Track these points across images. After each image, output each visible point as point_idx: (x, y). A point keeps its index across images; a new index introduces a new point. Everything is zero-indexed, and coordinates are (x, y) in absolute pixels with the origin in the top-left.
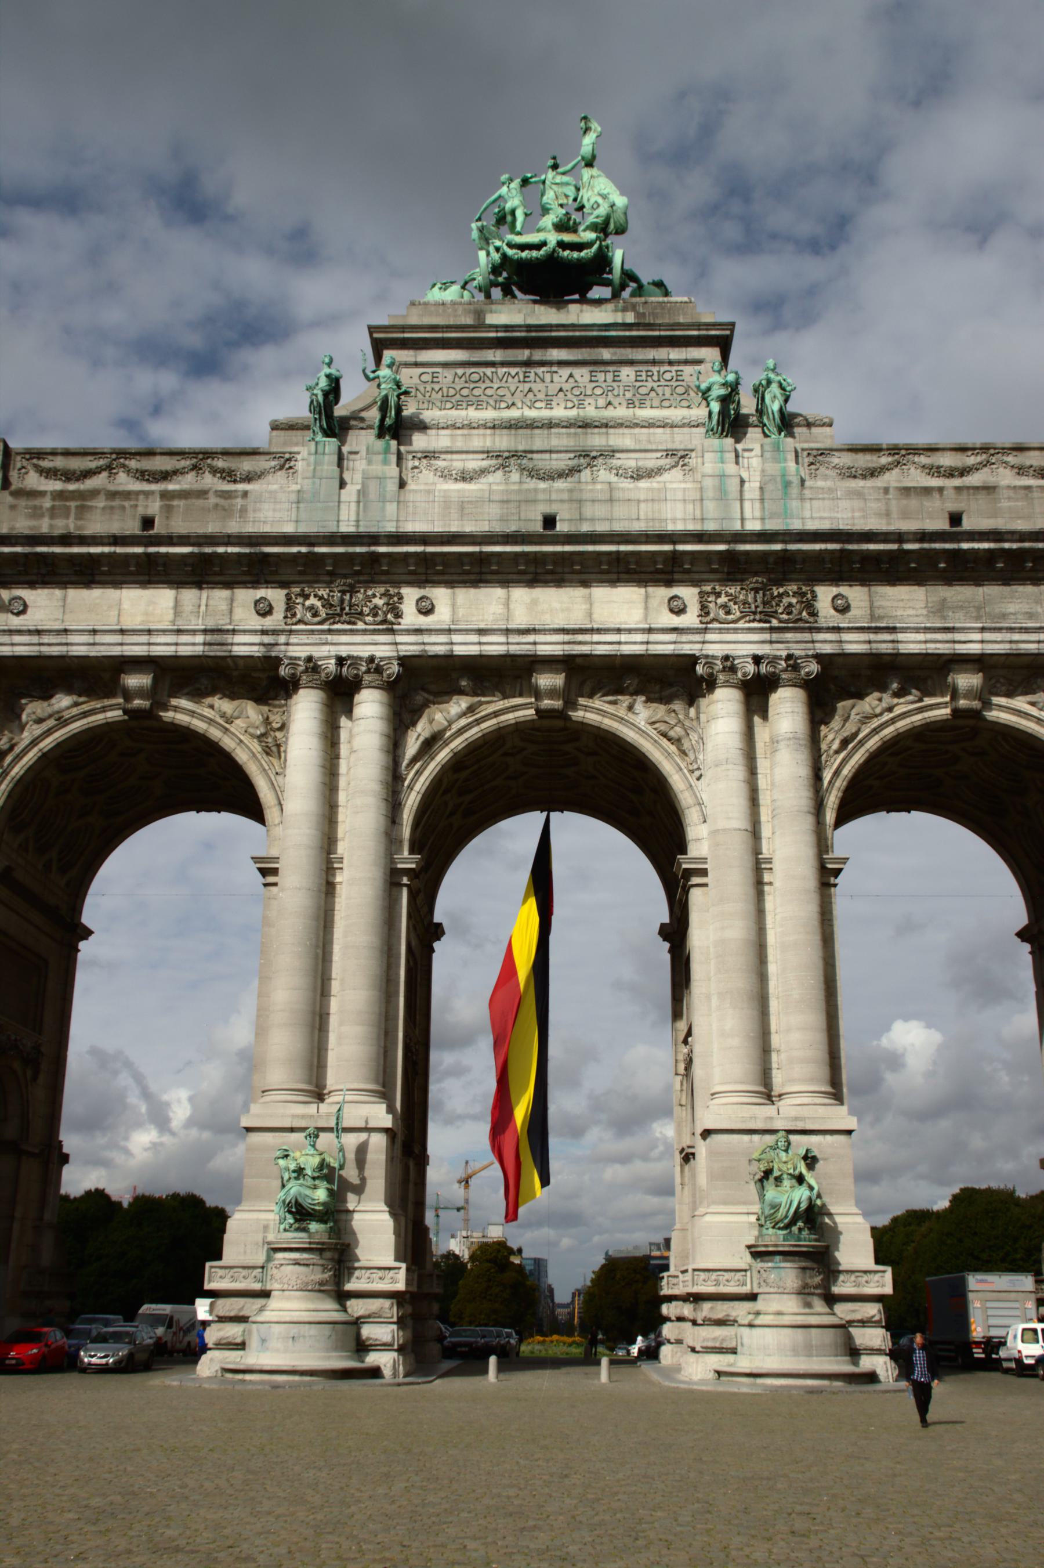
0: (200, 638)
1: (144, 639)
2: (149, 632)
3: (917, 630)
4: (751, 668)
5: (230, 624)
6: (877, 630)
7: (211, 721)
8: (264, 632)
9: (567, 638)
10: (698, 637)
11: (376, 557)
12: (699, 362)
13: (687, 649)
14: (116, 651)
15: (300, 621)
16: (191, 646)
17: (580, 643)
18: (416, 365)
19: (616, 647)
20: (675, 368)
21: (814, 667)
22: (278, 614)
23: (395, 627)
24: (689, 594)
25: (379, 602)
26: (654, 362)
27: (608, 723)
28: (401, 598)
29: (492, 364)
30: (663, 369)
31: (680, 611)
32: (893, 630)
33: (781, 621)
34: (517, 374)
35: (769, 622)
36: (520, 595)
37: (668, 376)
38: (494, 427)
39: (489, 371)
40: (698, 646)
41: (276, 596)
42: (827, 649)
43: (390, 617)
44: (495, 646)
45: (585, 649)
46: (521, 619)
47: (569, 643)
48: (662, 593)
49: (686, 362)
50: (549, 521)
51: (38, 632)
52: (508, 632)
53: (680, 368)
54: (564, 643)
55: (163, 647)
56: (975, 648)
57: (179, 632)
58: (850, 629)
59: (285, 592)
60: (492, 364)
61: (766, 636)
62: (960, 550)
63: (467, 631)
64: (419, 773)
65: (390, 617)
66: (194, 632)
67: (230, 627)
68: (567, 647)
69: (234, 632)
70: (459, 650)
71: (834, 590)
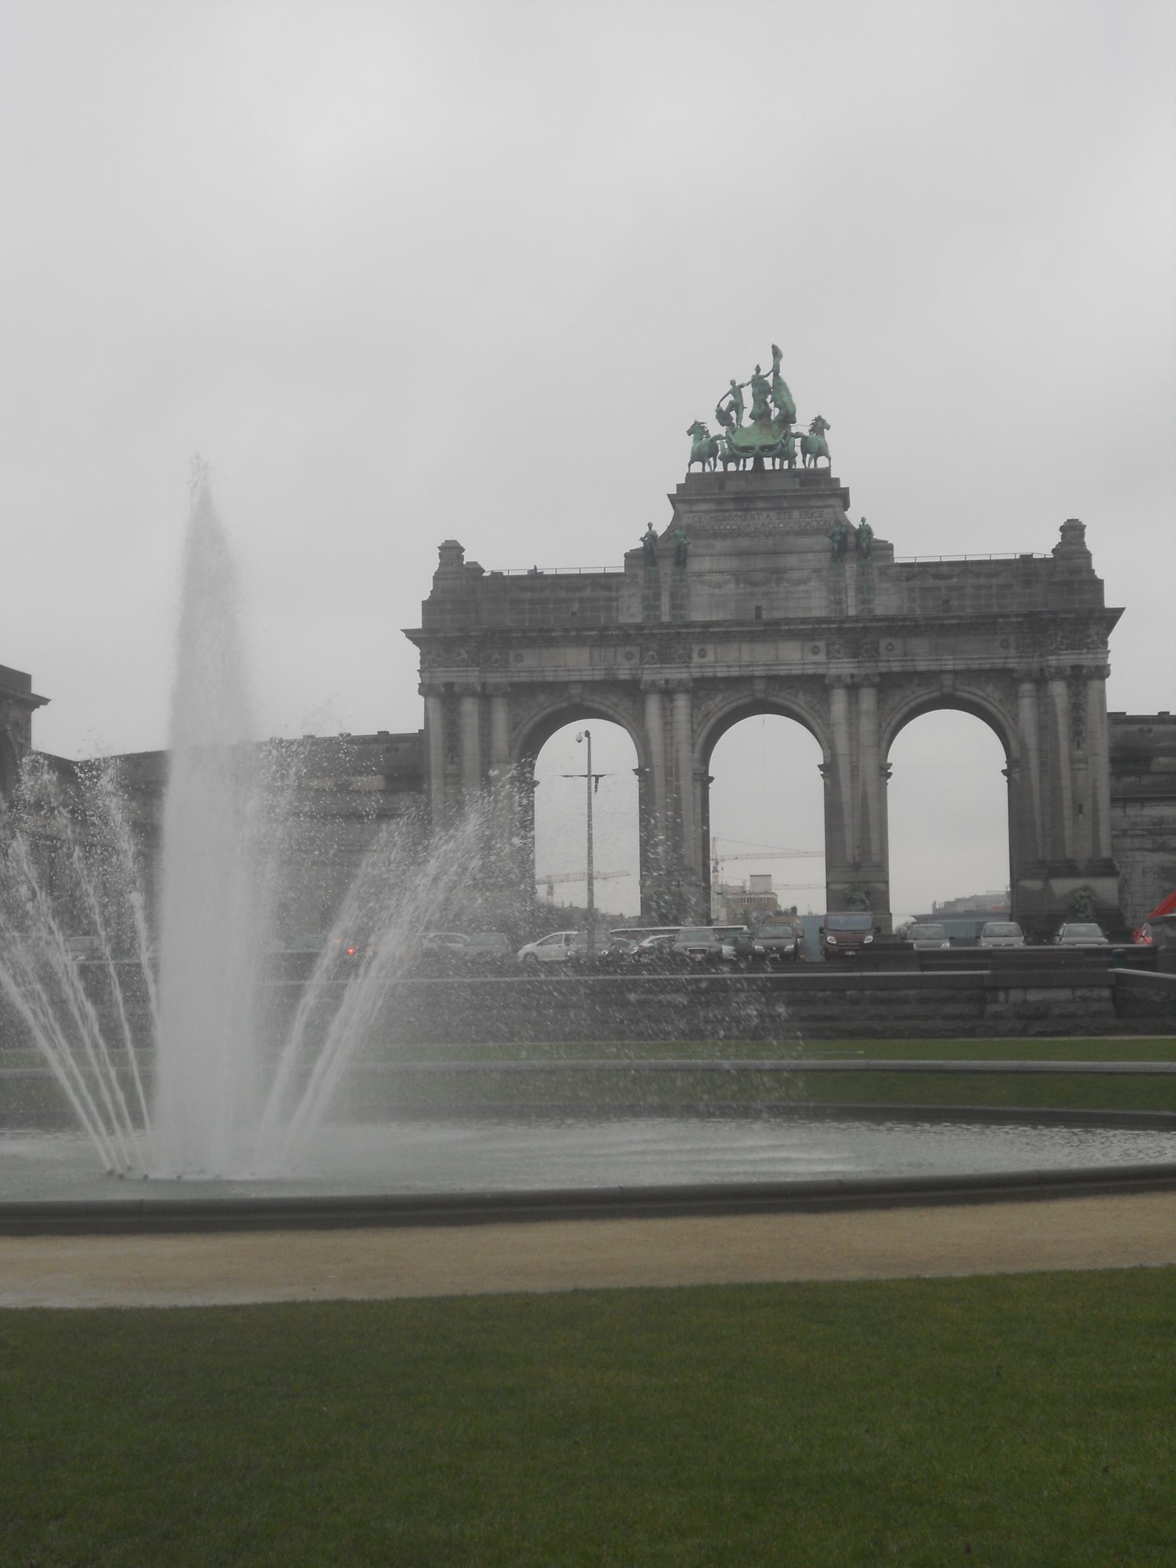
0: (603, 672)
1: (578, 673)
2: (581, 670)
3: (924, 660)
4: (849, 681)
5: (615, 664)
6: (906, 661)
7: (609, 707)
8: (631, 669)
9: (767, 668)
10: (825, 666)
11: (679, 634)
12: (831, 506)
13: (820, 671)
14: (566, 679)
15: (648, 663)
16: (598, 676)
17: (772, 670)
18: (691, 512)
19: (789, 671)
20: (820, 510)
21: (877, 679)
22: (636, 660)
23: (691, 665)
24: (821, 644)
25: (681, 652)
26: (810, 507)
27: (786, 703)
28: (691, 649)
29: (729, 510)
30: (813, 511)
31: (816, 653)
32: (913, 660)
33: (863, 657)
34: (741, 515)
35: (857, 658)
36: (746, 647)
37: (816, 515)
38: (731, 555)
39: (727, 514)
40: (825, 670)
41: (635, 650)
42: (884, 670)
43: (687, 659)
44: (735, 672)
45: (775, 673)
46: (746, 658)
47: (768, 670)
48: (810, 644)
49: (825, 507)
50: (758, 609)
51: (531, 671)
52: (740, 666)
53: (823, 509)
54: (765, 670)
55: (587, 677)
56: (950, 667)
57: (593, 670)
58: (895, 661)
59: (639, 648)
60: (729, 510)
61: (856, 665)
62: (943, 625)
63: (722, 666)
64: (702, 729)
65: (687, 659)
66: (600, 670)
67: (616, 667)
68: (767, 672)
69: (618, 669)
70: (719, 675)
71: (888, 640)
